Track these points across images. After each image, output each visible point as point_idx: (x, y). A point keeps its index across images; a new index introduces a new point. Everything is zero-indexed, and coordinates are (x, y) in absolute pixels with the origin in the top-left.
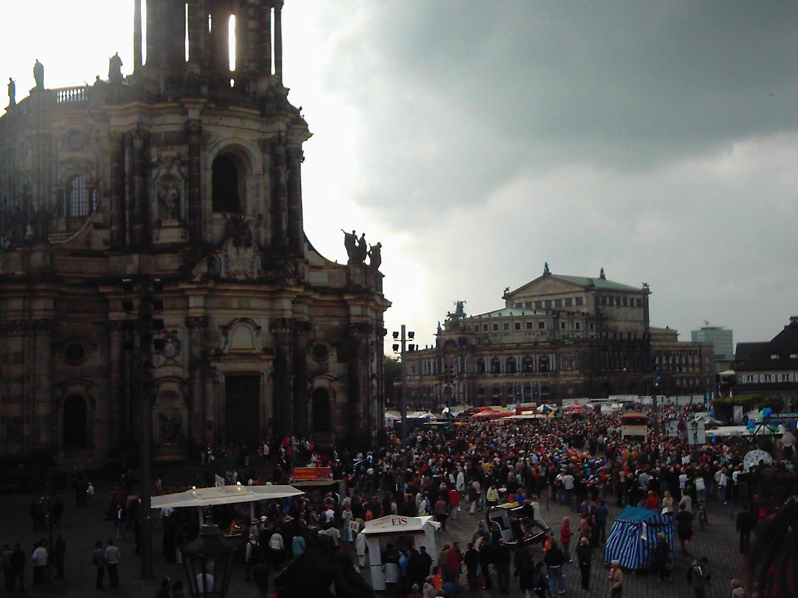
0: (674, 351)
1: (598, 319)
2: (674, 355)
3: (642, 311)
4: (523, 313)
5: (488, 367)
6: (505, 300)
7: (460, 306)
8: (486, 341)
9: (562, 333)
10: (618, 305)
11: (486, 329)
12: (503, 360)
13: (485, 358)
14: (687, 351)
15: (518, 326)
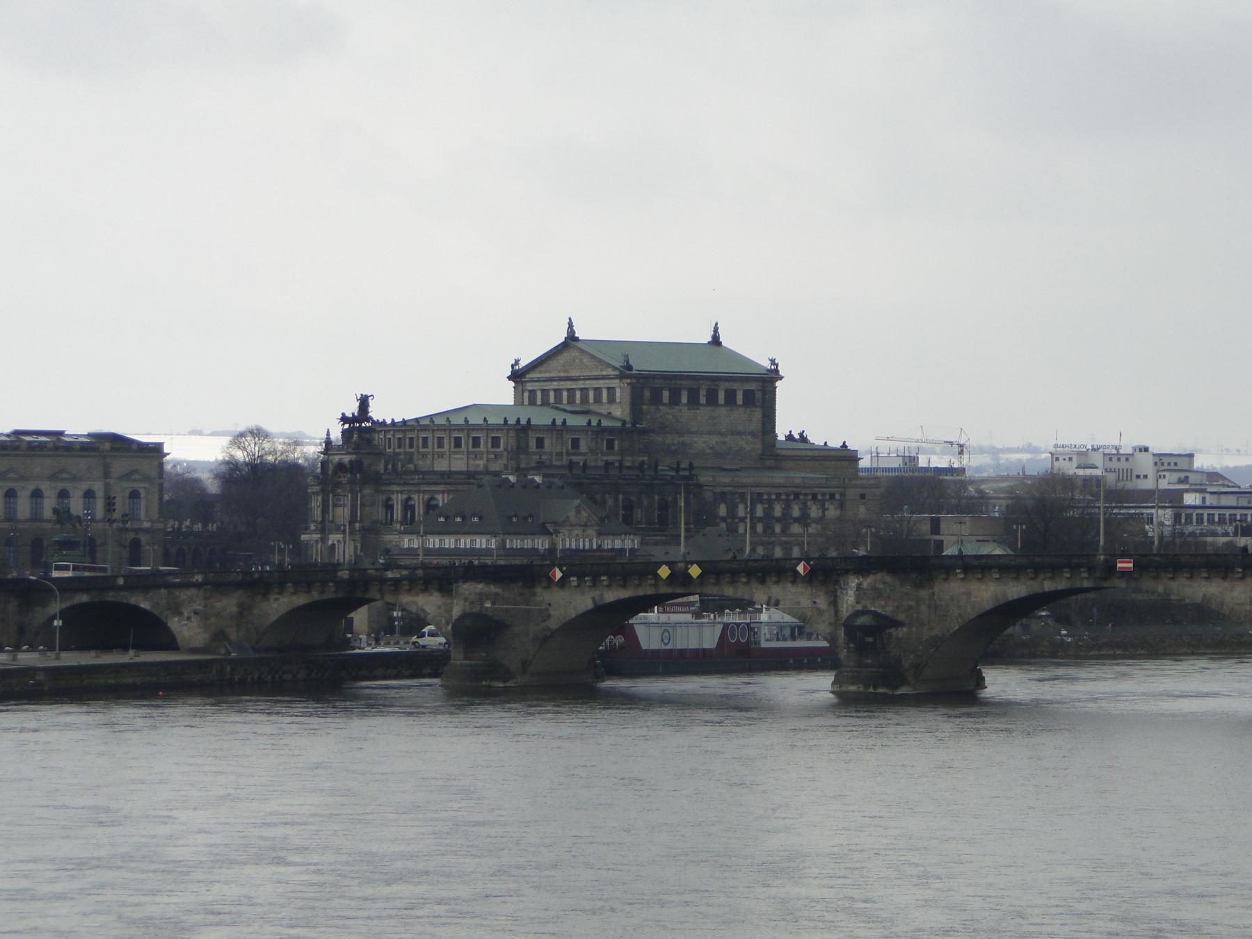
0: (769, 494)
1: (631, 432)
2: (770, 502)
3: (758, 414)
4: (466, 420)
5: (398, 513)
6: (512, 384)
7: (364, 402)
8: (411, 466)
9: (536, 457)
10: (694, 401)
11: (411, 446)
12: (418, 501)
13: (394, 497)
14: (806, 495)
15: (458, 442)
